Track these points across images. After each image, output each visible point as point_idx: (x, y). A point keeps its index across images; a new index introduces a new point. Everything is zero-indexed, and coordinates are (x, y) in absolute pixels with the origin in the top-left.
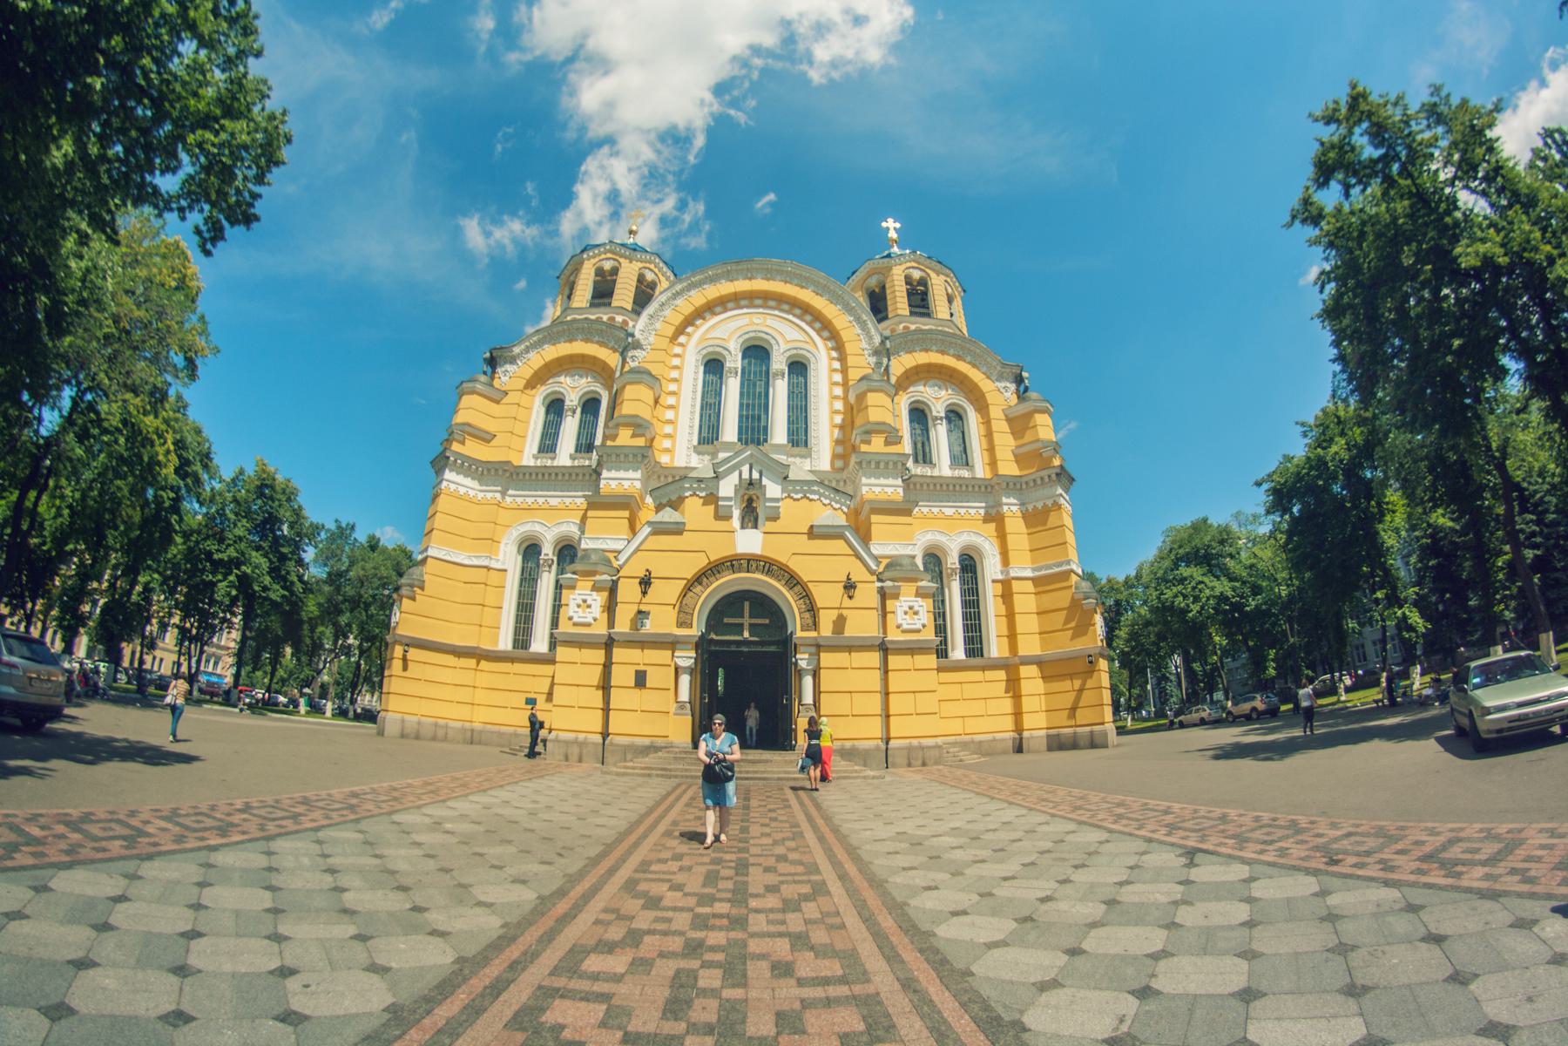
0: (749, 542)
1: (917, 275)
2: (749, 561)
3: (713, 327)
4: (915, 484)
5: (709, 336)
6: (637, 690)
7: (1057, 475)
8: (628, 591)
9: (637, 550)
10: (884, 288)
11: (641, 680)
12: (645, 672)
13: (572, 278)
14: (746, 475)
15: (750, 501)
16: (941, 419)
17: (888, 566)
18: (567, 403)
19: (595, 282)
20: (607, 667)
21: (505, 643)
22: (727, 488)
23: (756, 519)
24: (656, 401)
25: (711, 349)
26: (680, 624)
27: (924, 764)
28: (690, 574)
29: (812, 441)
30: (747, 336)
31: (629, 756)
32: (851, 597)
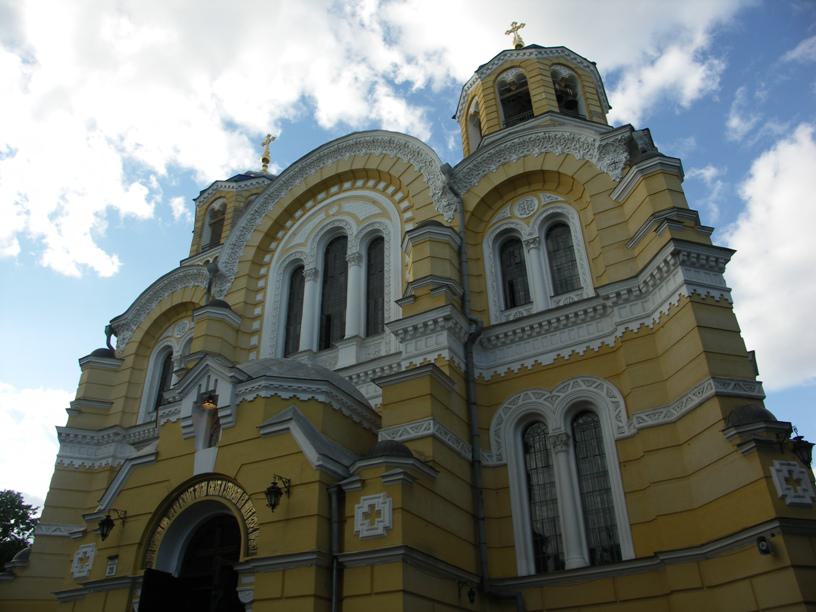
4: (497, 337)
7: (675, 254)
14: (203, 390)
16: (535, 239)
18: (175, 354)
24: (238, 331)
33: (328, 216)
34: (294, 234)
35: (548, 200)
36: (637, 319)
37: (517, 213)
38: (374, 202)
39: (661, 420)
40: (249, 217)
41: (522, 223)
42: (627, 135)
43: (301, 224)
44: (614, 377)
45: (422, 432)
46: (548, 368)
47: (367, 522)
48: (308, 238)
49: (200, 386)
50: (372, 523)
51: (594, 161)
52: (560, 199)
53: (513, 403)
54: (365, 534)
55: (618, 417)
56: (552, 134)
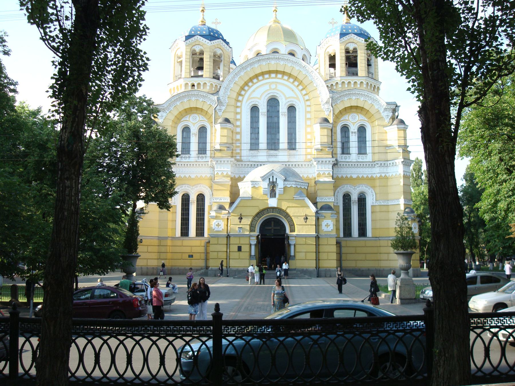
0: (273, 203)
2: (273, 209)
6: (238, 253)
7: (402, 162)
9: (236, 207)
11: (240, 249)
12: (241, 247)
14: (271, 180)
15: (273, 187)
16: (355, 132)
17: (322, 208)
20: (228, 245)
21: (178, 233)
23: (275, 194)
27: (330, 276)
28: (254, 214)
30: (269, 95)
31: (237, 273)
33: (270, 89)
35: (362, 119)
36: (384, 173)
37: (350, 119)
39: (385, 204)
40: (233, 76)
41: (351, 123)
42: (394, 107)
43: (257, 87)
44: (374, 187)
45: (331, 200)
48: (261, 96)
49: (269, 179)
50: (327, 228)
51: (381, 111)
52: (366, 119)
53: (343, 187)
55: (373, 199)
56: (370, 96)
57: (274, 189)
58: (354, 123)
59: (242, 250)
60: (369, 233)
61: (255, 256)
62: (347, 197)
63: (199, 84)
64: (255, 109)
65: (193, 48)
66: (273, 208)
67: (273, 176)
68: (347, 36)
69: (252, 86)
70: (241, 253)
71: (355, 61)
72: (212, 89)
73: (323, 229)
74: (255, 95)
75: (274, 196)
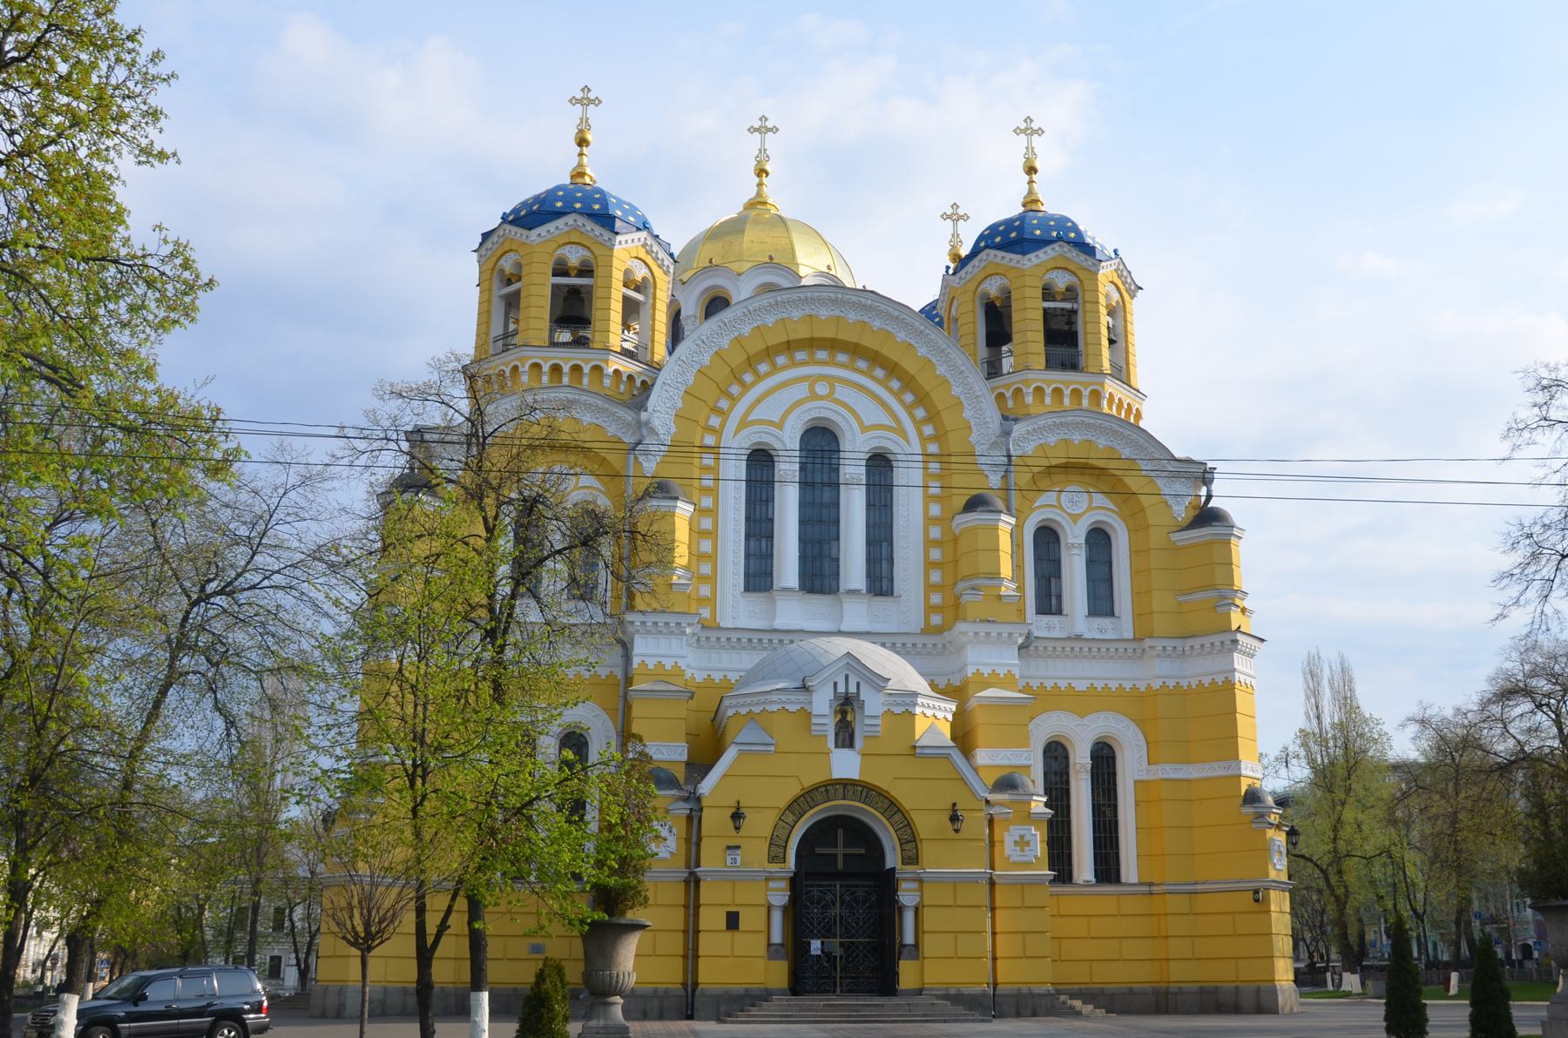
0: (846, 765)
1: (1061, 281)
3: (758, 401)
4: (1036, 647)
5: (749, 419)
6: (729, 934)
8: (714, 821)
10: (1008, 298)
11: (733, 921)
12: (738, 913)
13: (507, 264)
14: (841, 689)
15: (844, 713)
19: (554, 286)
22: (822, 704)
23: (852, 736)
25: (756, 438)
26: (772, 859)
27: (1034, 1014)
29: (898, 586)
32: (957, 831)
33: (814, 396)
34: (758, 401)
37: (1063, 504)
38: (884, 404)
46: (1080, 694)
47: (1018, 848)
49: (835, 684)
50: (1022, 850)
52: (1112, 506)
54: (1014, 858)
57: (849, 718)
58: (1075, 518)
59: (742, 926)
60: (1130, 870)
61: (782, 945)
62: (1056, 754)
63: (576, 369)
64: (761, 461)
65: (558, 252)
66: (846, 784)
67: (847, 677)
68: (1048, 249)
69: (754, 384)
70: (737, 935)
71: (1066, 328)
72: (618, 388)
73: (1007, 853)
74: (765, 411)
75: (847, 741)
